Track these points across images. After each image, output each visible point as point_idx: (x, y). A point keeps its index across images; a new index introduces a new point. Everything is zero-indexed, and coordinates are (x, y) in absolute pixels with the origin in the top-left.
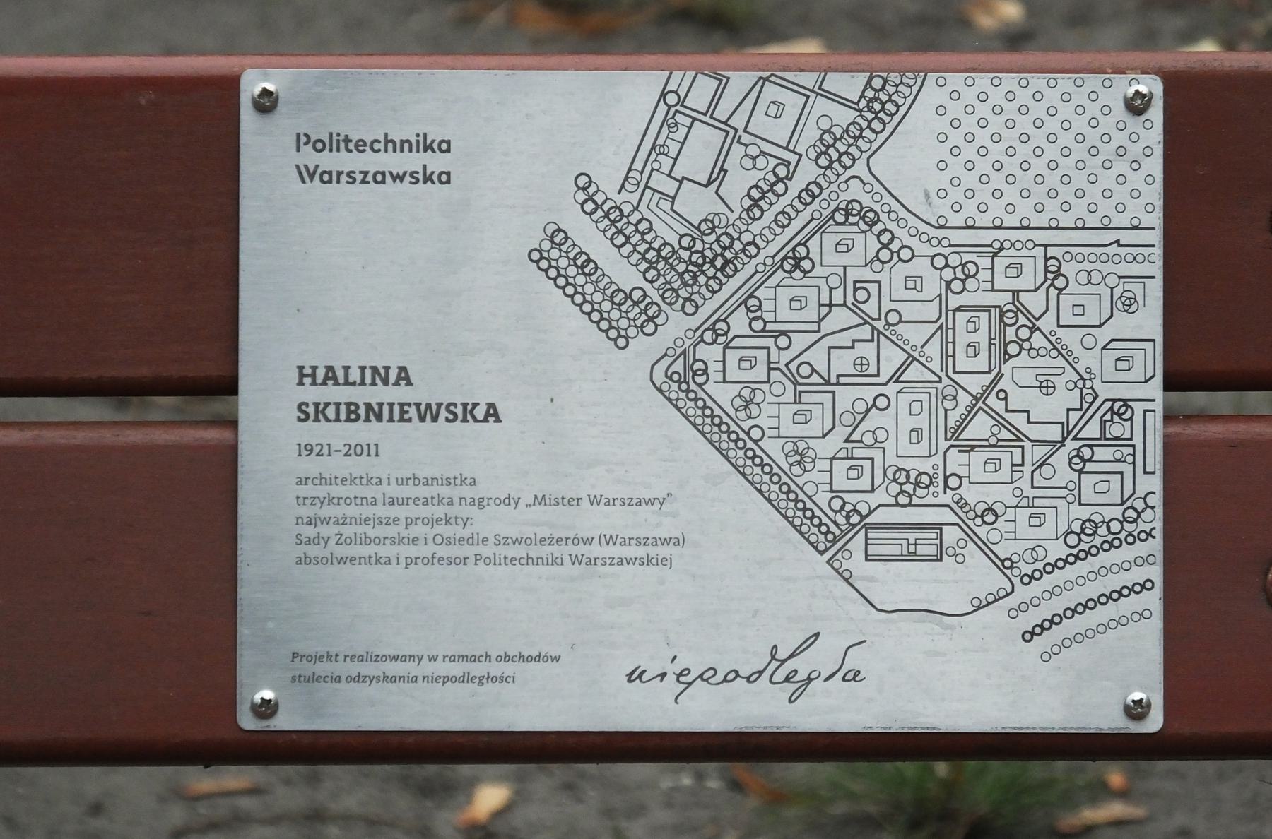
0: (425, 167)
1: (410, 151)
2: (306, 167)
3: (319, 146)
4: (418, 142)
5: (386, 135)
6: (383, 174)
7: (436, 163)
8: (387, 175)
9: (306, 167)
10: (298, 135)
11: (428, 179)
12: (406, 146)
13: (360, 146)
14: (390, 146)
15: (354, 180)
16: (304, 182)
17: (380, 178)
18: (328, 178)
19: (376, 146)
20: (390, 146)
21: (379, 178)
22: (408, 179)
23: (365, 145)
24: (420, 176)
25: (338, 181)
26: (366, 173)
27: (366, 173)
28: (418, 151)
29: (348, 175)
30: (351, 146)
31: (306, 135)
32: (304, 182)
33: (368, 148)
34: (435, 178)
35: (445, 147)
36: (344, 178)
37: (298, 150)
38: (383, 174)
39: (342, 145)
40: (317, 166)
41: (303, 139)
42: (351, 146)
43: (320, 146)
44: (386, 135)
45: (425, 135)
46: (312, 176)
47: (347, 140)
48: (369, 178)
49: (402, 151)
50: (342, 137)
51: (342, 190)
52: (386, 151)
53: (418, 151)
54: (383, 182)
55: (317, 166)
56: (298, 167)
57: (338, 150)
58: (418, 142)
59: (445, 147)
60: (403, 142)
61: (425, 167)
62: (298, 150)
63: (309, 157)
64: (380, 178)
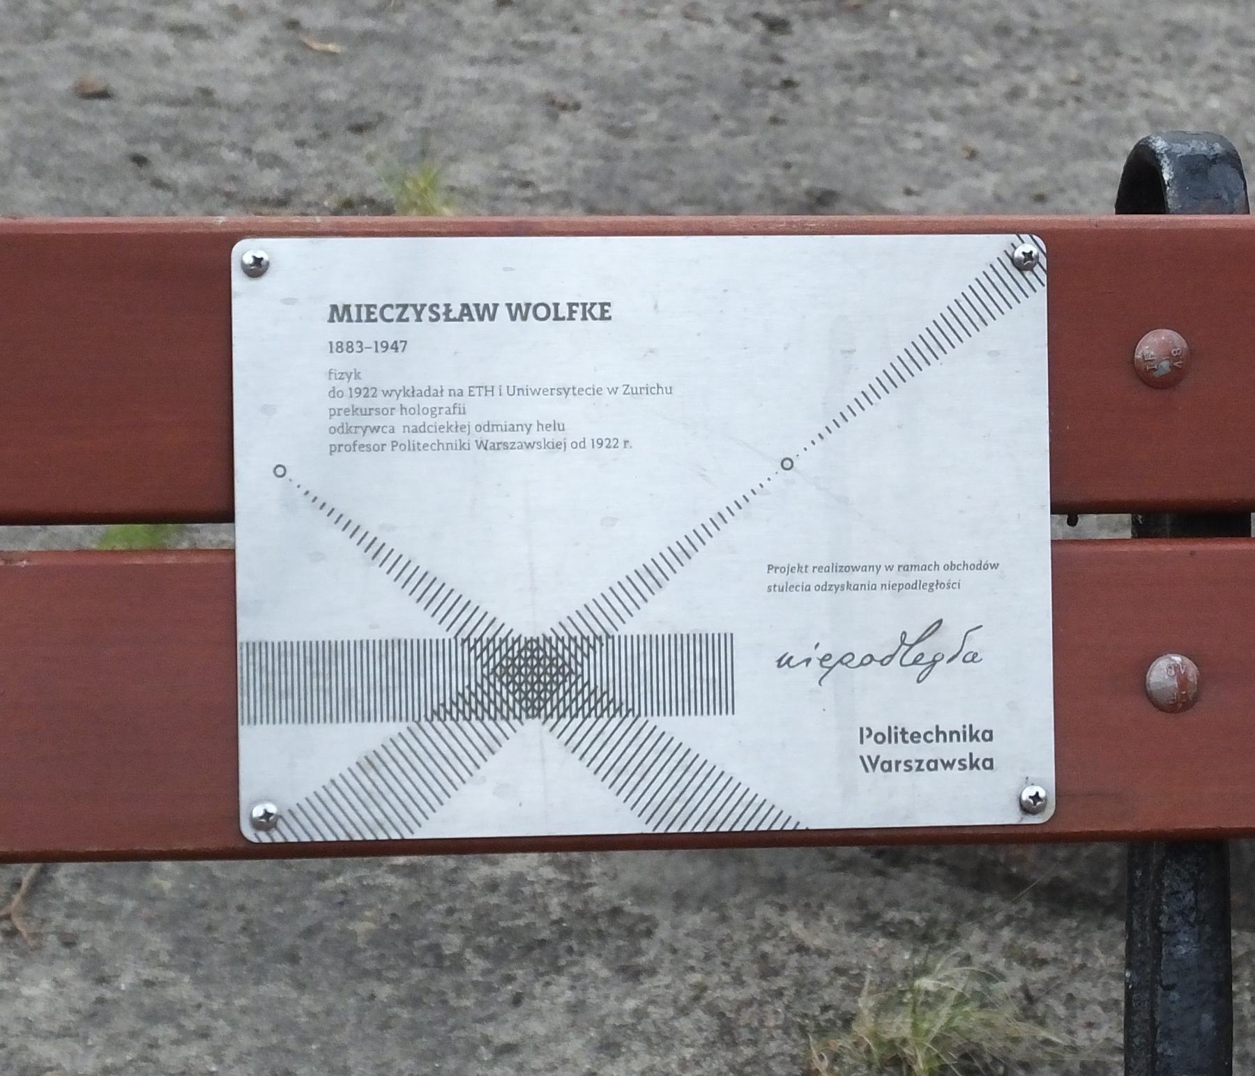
0: (971, 755)
1: (958, 739)
2: (869, 757)
3: (880, 738)
4: (965, 733)
5: (937, 727)
6: (936, 762)
7: (980, 750)
8: (940, 763)
9: (869, 757)
10: (862, 729)
11: (974, 765)
12: (955, 736)
13: (915, 737)
14: (941, 736)
15: (911, 768)
16: (867, 770)
17: (933, 765)
18: (888, 766)
19: (929, 737)
20: (941, 736)
21: (932, 765)
22: (957, 765)
23: (919, 736)
24: (967, 763)
25: (897, 769)
26: (920, 762)
27: (920, 762)
28: (965, 739)
29: (906, 763)
30: (907, 737)
31: (869, 729)
32: (867, 770)
33: (922, 739)
34: (980, 764)
35: (989, 736)
36: (902, 766)
37: (862, 742)
38: (936, 762)
39: (900, 736)
40: (878, 757)
41: (866, 733)
42: (907, 737)
43: (881, 738)
44: (937, 727)
45: (971, 726)
46: (874, 766)
47: (904, 732)
48: (924, 766)
49: (951, 740)
50: (899, 730)
51: (901, 776)
52: (938, 740)
53: (965, 739)
54: (936, 768)
55: (878, 757)
56: (862, 758)
57: (896, 741)
58: (965, 733)
59: (989, 736)
60: (951, 733)
61: (971, 755)
62: (862, 742)
63: (870, 748)
64: (933, 765)
